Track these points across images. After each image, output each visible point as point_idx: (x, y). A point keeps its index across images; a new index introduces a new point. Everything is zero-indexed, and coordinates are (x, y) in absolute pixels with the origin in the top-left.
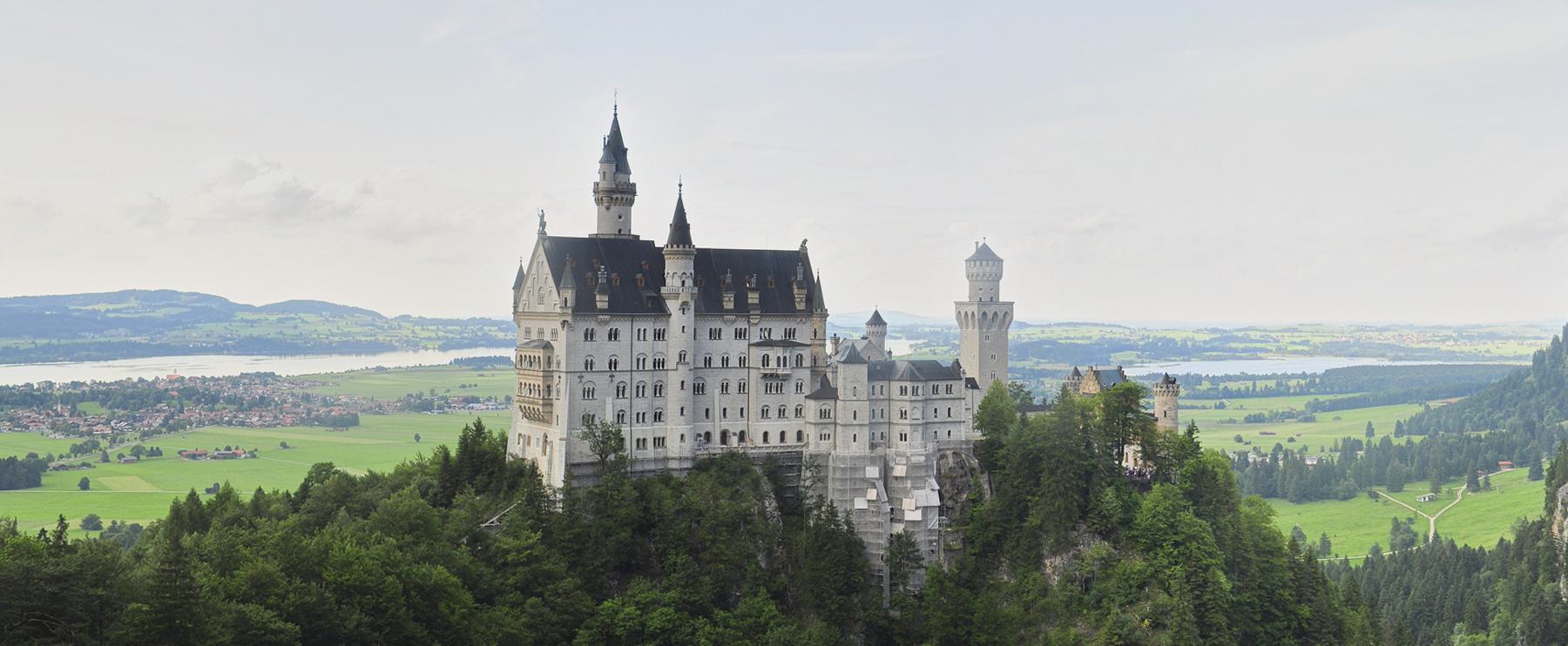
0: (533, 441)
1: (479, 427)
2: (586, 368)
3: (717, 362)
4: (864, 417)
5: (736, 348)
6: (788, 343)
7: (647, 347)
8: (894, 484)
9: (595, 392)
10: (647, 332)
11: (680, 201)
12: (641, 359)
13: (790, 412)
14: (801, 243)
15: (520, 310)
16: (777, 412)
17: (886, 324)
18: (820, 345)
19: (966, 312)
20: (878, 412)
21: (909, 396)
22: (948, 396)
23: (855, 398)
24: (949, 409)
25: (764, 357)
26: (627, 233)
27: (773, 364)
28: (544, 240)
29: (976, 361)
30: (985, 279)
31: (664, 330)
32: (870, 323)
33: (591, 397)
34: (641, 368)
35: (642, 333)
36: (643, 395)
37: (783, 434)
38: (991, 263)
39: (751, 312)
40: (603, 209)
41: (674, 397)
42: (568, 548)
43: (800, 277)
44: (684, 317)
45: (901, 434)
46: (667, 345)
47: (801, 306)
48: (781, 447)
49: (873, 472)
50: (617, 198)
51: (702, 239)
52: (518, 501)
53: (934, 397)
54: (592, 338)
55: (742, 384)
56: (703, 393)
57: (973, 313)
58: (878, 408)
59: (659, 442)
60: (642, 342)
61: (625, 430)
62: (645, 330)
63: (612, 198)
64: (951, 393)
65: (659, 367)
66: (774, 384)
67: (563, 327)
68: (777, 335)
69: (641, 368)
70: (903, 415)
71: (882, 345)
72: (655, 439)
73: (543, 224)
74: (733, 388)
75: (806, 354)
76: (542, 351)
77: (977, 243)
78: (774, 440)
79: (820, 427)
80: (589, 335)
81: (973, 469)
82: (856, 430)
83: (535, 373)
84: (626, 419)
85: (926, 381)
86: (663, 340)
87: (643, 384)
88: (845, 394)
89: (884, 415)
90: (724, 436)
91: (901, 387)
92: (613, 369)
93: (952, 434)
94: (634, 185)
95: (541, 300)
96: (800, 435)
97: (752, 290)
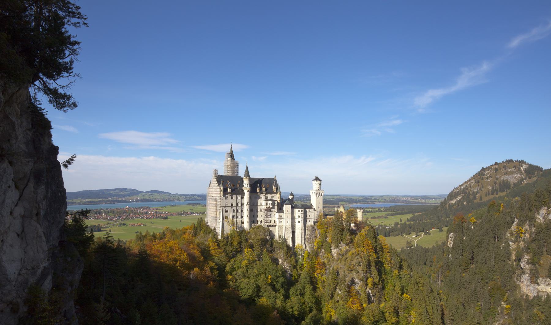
1: (201, 219)
11: (247, 167)
21: (300, 212)
27: (268, 205)
28: (216, 176)
38: (318, 181)
41: (246, 212)
43: (275, 184)
47: (275, 191)
52: (211, 236)
59: (242, 223)
70: (299, 217)
75: (276, 202)
80: (226, 198)
82: (288, 220)
84: (235, 217)
88: (285, 212)
96: (275, 221)
97: (264, 188)
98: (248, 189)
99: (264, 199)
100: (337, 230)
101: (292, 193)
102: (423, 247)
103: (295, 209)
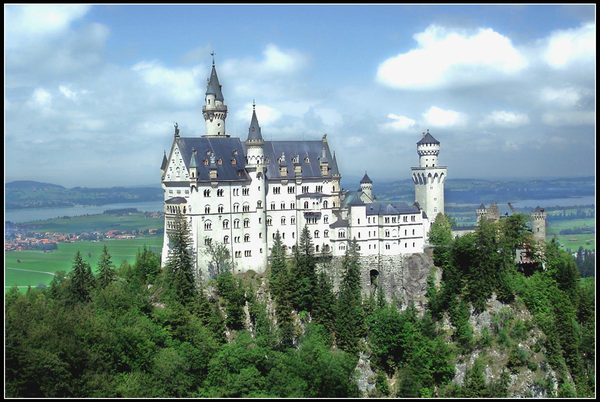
3: (278, 207)
6: (318, 195)
7: (241, 199)
12: (236, 205)
13: (321, 234)
19: (418, 174)
20: (372, 234)
25: (305, 203)
26: (223, 134)
27: (310, 206)
34: (236, 212)
35: (236, 190)
36: (238, 228)
41: (255, 227)
45: (386, 246)
47: (325, 172)
50: (217, 114)
54: (208, 195)
55: (293, 219)
58: (372, 229)
59: (248, 253)
61: (228, 247)
62: (237, 189)
64: (414, 221)
65: (246, 210)
72: (245, 252)
73: (177, 131)
74: (288, 221)
79: (339, 242)
80: (207, 193)
84: (229, 240)
91: (386, 218)
92: (221, 212)
98: (260, 169)
101: (366, 176)
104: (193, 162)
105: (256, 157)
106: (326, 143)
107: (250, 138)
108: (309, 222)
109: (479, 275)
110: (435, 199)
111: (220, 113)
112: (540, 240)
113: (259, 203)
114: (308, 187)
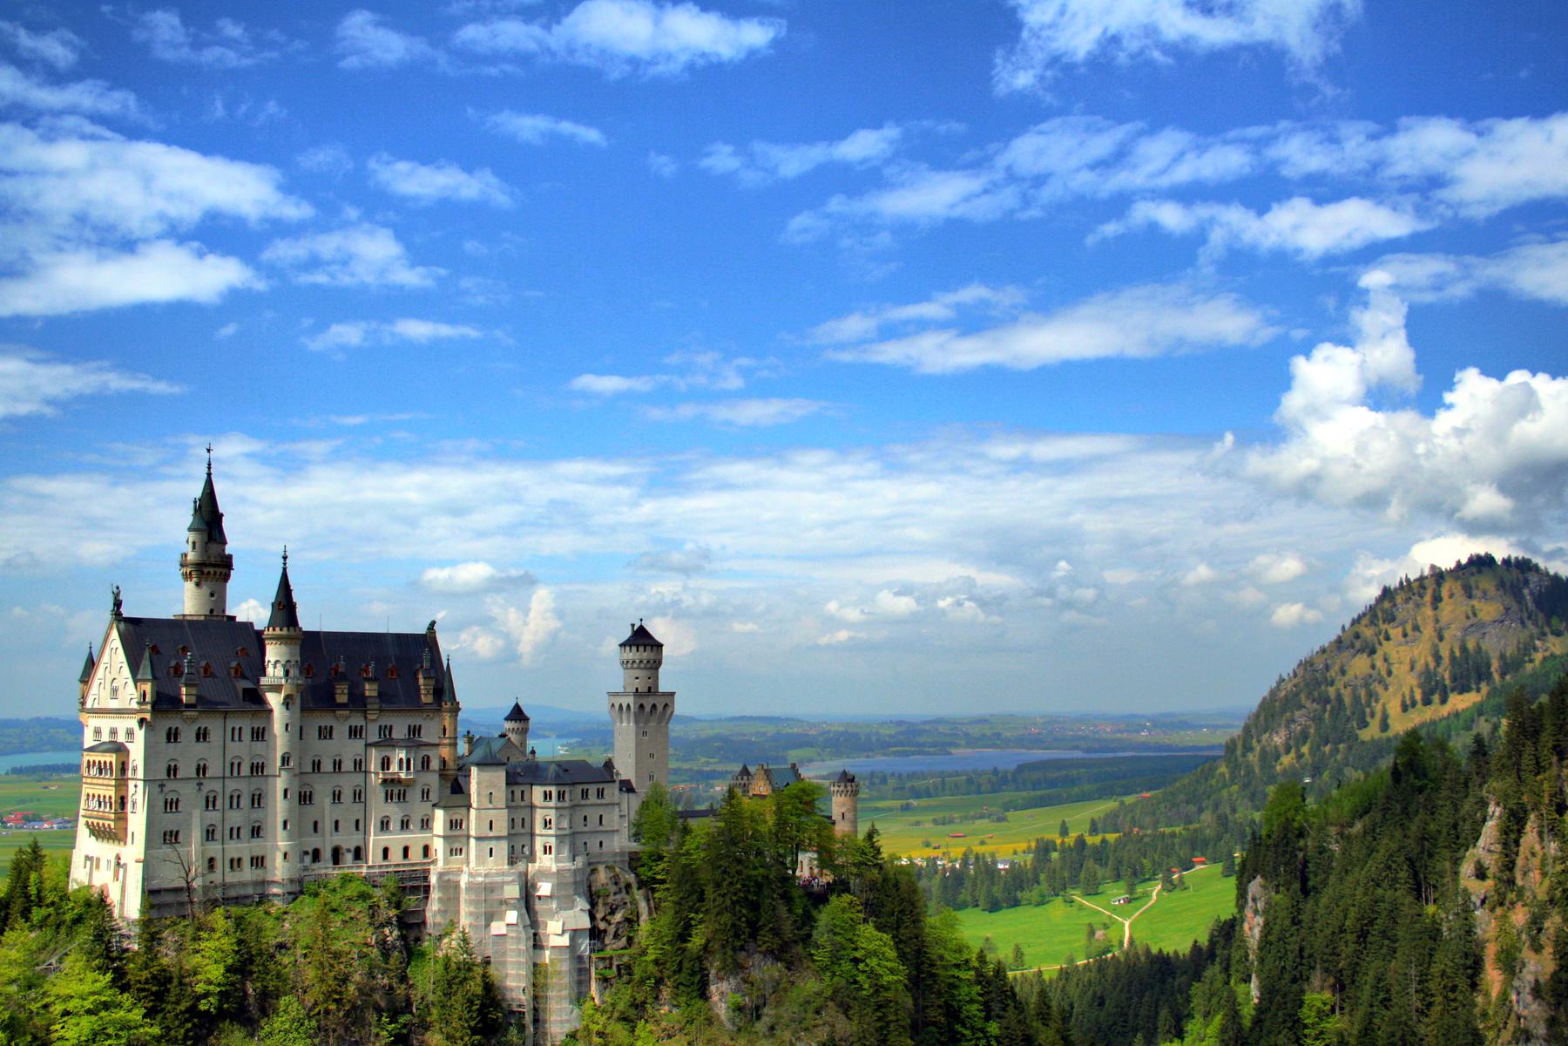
0: (103, 864)
2: (169, 775)
3: (327, 766)
4: (502, 828)
5: (356, 747)
8: (539, 906)
9: (180, 804)
10: (243, 731)
11: (285, 577)
12: (236, 762)
14: (427, 624)
15: (89, 705)
16: (399, 824)
17: (526, 719)
18: (450, 745)
19: (621, 706)
20: (518, 822)
22: (599, 801)
23: (491, 806)
24: (601, 816)
25: (383, 759)
27: (394, 768)
28: (119, 621)
29: (632, 761)
30: (642, 666)
31: (264, 728)
32: (508, 719)
33: (174, 810)
34: (235, 774)
35: (237, 732)
36: (238, 806)
37: (406, 850)
38: (648, 648)
39: (369, 707)
40: (190, 586)
41: (279, 808)
42: (144, 990)
43: (426, 665)
44: (287, 713)
45: (545, 847)
46: (267, 746)
48: (404, 865)
49: (513, 891)
50: (209, 573)
51: (308, 621)
53: (583, 802)
56: (311, 803)
57: (628, 706)
59: (258, 862)
60: (238, 743)
62: (240, 729)
63: (203, 573)
66: (396, 791)
67: (141, 727)
68: (400, 732)
69: (235, 774)
70: (547, 824)
71: (523, 743)
72: (252, 859)
73: (118, 604)
74: (347, 796)
75: (432, 753)
76: (114, 755)
77: (633, 625)
78: (396, 856)
80: (172, 736)
81: (628, 886)
82: (493, 844)
83: (106, 782)
84: (218, 835)
85: (574, 784)
86: (263, 740)
87: (238, 793)
89: (525, 825)
90: (337, 855)
91: (545, 792)
92: (201, 775)
93: (604, 845)
94: (230, 557)
95: (115, 691)
99: (374, 738)
100: (731, 884)
102: (1154, 951)
103: (526, 788)
104: (145, 670)
105: (283, 663)
106: (435, 638)
107: (272, 623)
108: (392, 799)
109: (723, 906)
110: (652, 756)
111: (216, 569)
112: (844, 836)
113: (285, 760)
114: (391, 727)
